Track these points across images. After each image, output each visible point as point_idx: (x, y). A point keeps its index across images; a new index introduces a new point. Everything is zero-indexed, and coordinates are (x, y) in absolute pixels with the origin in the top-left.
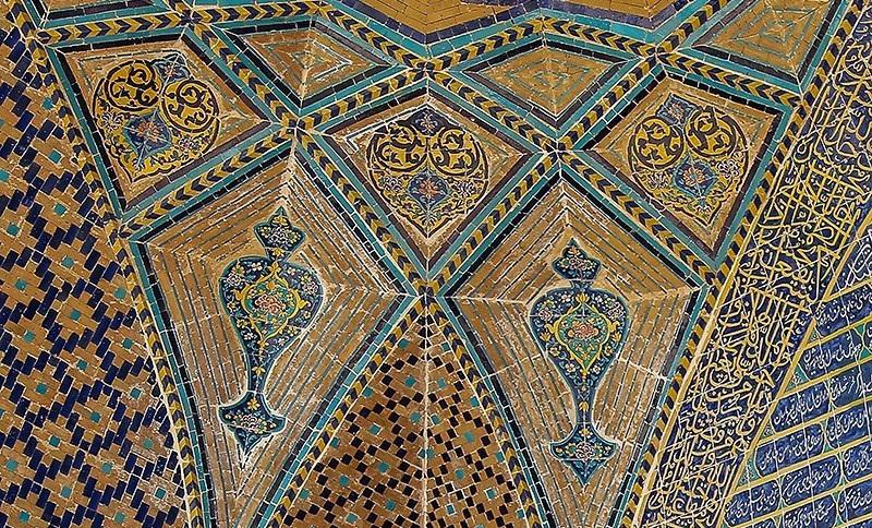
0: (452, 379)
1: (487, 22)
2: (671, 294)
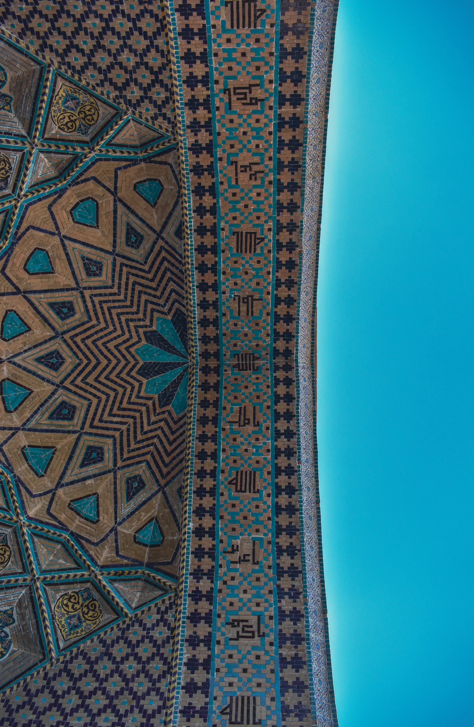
1: (18, 228)
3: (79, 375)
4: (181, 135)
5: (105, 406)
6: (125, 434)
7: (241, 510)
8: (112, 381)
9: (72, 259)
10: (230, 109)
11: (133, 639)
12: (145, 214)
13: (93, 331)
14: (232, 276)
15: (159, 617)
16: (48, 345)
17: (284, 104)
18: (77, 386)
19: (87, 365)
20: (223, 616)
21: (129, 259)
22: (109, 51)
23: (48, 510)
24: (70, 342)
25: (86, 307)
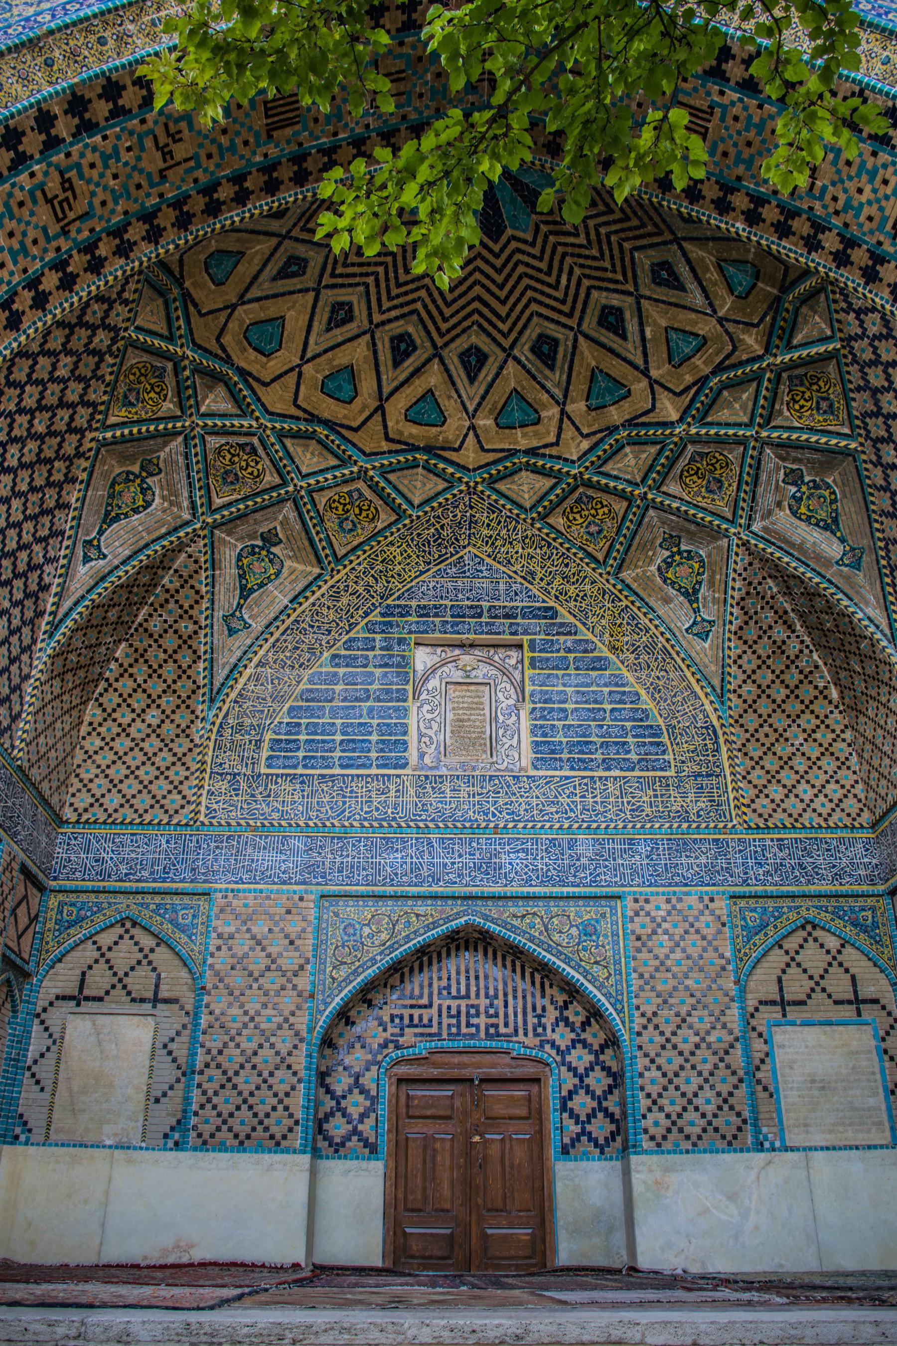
0: (193, 567)
1: (298, 419)
2: (309, 569)
3: (495, 327)
4: (141, 263)
5: (543, 293)
6: (587, 272)
7: (735, 145)
8: (506, 280)
9: (330, 344)
10: (87, 213)
11: (868, 355)
12: (256, 261)
13: (431, 307)
14: (340, 121)
15: (852, 315)
16: (452, 368)
17: (57, 136)
18: (511, 330)
19: (481, 315)
20: (882, 239)
21: (324, 268)
22: (62, 391)
23: (675, 393)
24: (448, 337)
25: (397, 318)
